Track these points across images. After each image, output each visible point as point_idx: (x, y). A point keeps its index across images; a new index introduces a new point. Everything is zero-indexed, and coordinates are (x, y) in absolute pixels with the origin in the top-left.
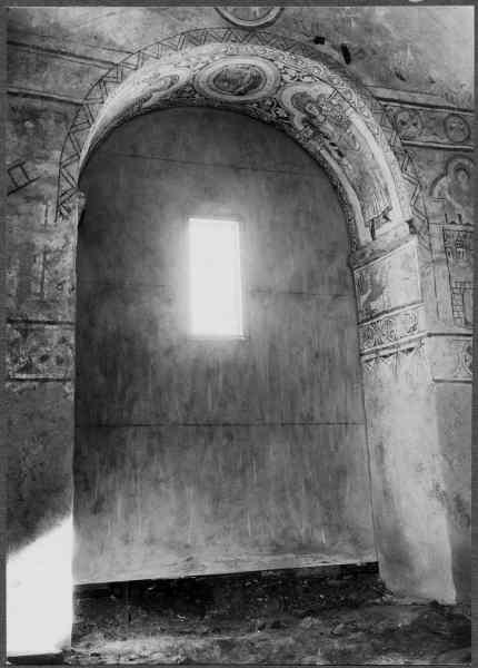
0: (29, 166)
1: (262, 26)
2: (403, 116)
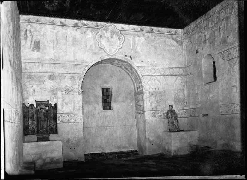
0: (73, 87)
1: (114, 54)
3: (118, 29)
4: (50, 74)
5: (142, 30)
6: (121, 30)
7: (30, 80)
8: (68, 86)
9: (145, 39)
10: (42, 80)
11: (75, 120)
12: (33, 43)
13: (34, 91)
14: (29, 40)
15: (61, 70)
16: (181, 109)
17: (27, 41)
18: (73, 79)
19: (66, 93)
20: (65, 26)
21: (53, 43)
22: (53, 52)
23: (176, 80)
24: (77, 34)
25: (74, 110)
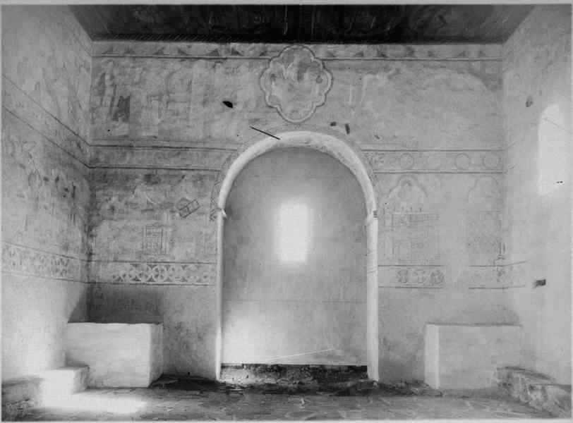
0: (200, 201)
1: (304, 121)
2: (377, 158)
3: (317, 58)
4: (147, 172)
5: (383, 56)
6: (325, 60)
7: (106, 184)
8: (187, 198)
9: (390, 77)
10: (129, 184)
11: (199, 281)
12: (117, 101)
13: (113, 209)
14: (109, 96)
15: (173, 163)
16: (486, 263)
17: (104, 98)
18: (199, 182)
19: (181, 215)
20: (187, 60)
21: (160, 100)
22: (157, 120)
23: (475, 187)
24: (218, 77)
25: (196, 255)
